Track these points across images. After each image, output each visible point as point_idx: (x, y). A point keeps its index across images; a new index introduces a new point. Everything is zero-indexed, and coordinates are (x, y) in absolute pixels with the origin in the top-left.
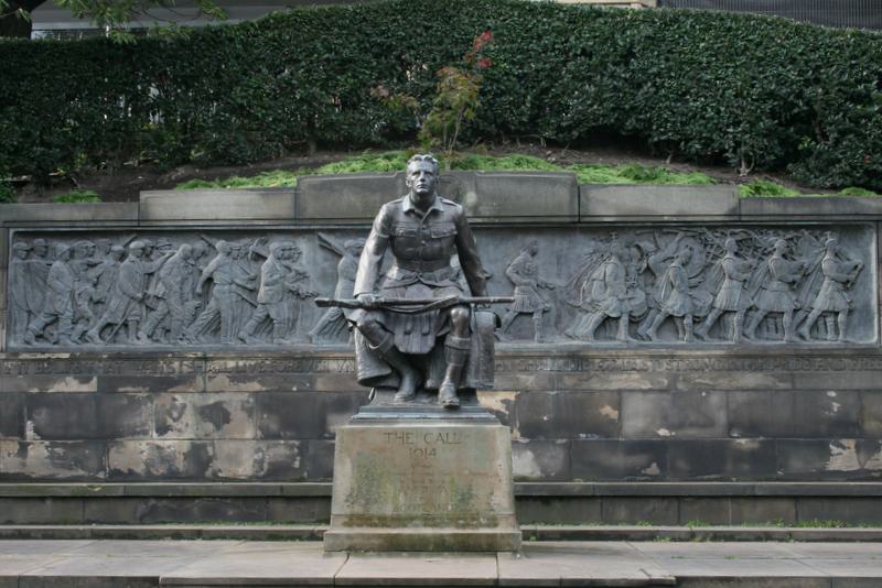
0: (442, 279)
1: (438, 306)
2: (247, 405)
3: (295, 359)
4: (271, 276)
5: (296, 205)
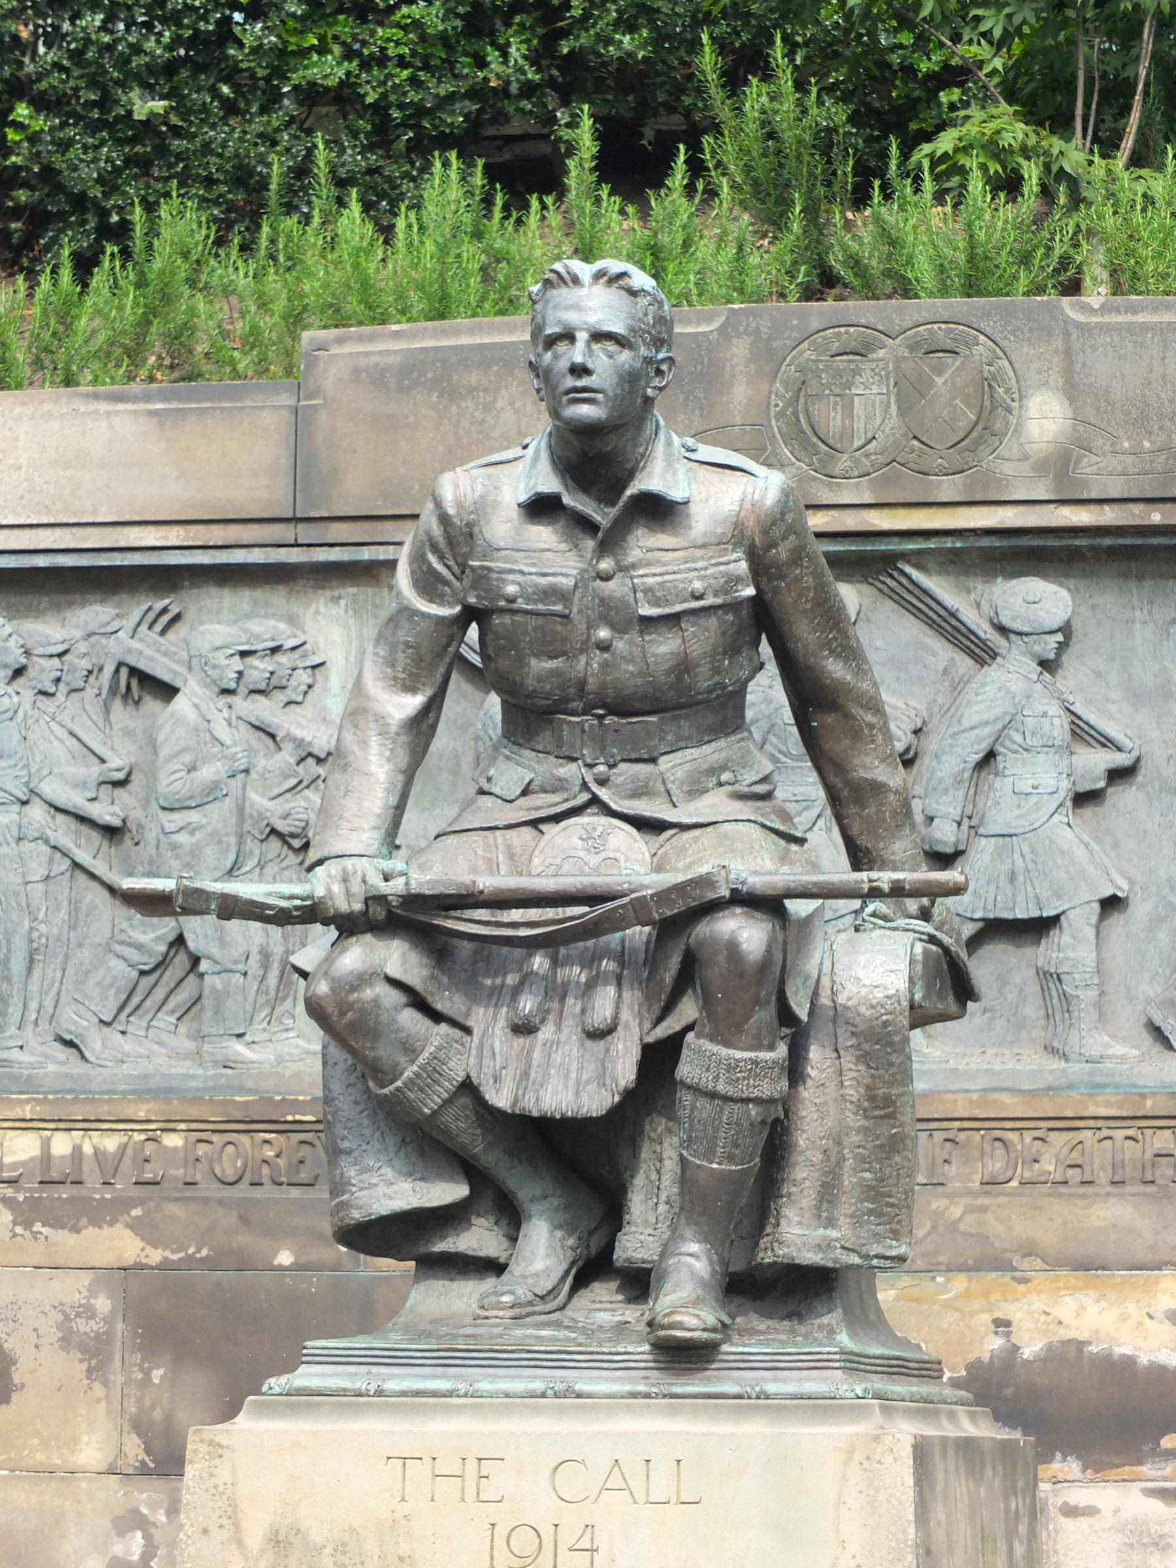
0: (696, 791)
1: (639, 911)
2: (83, 1326)
3: (287, 1129)
4: (192, 769)
5: (302, 464)
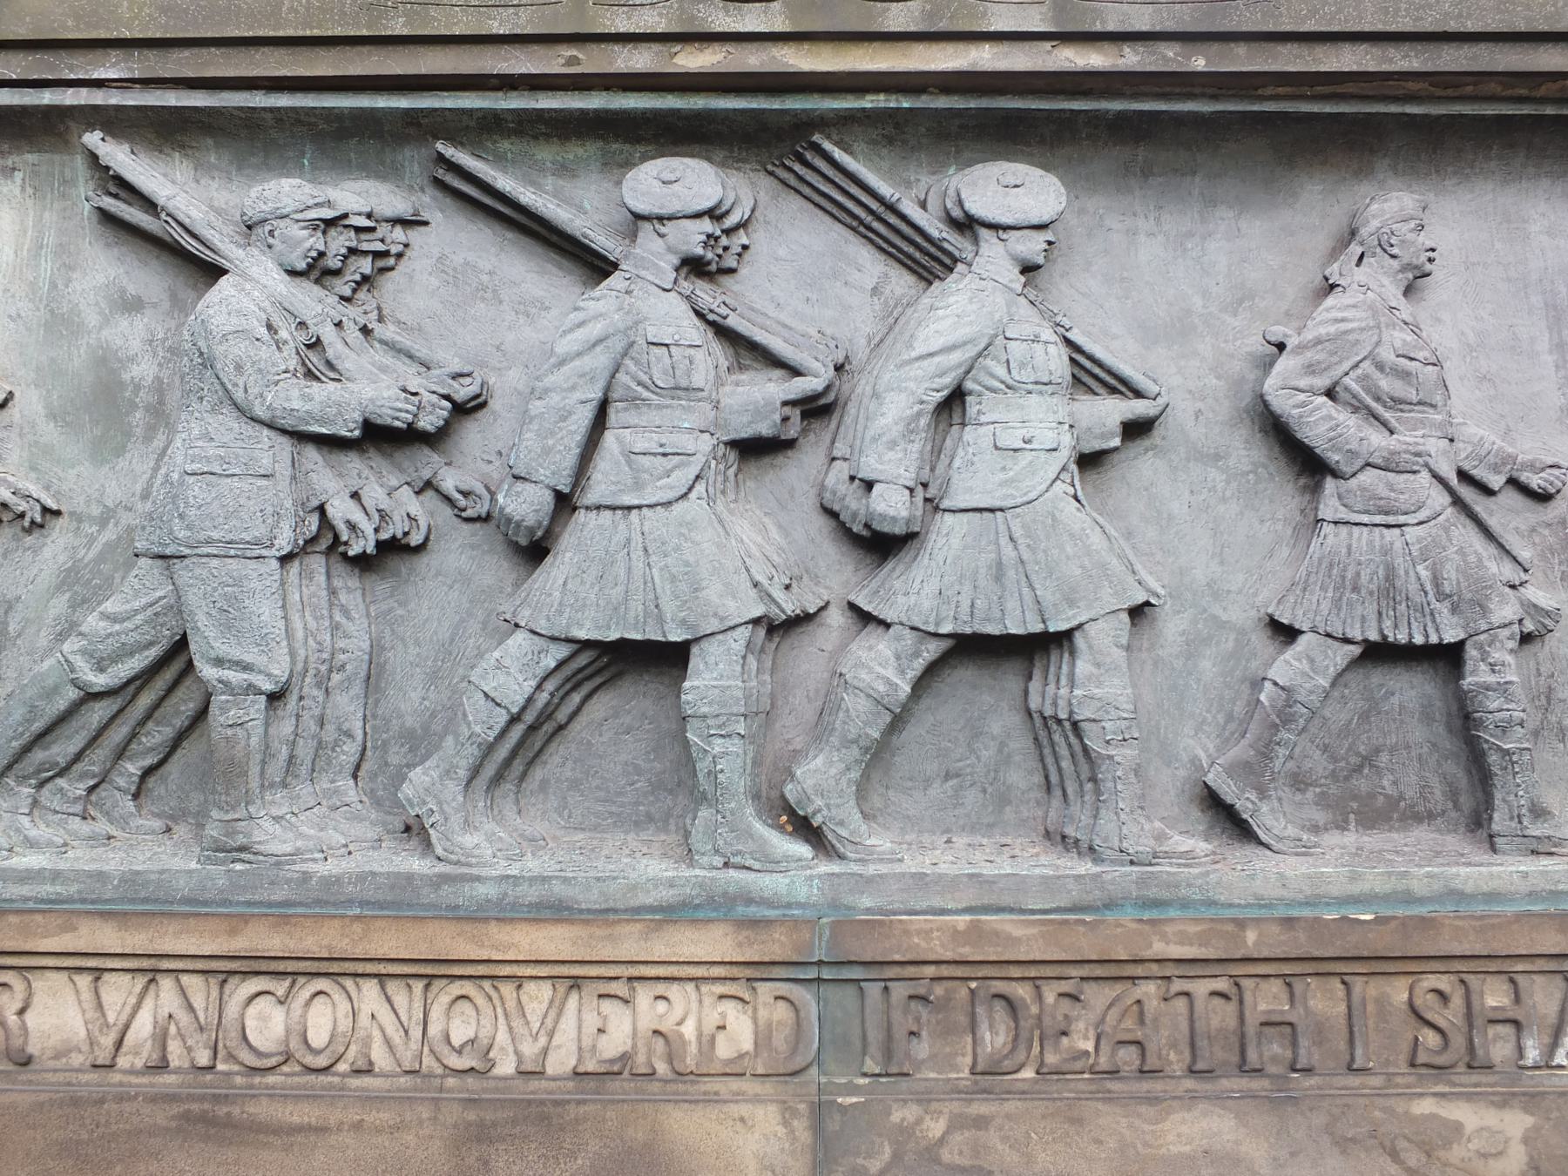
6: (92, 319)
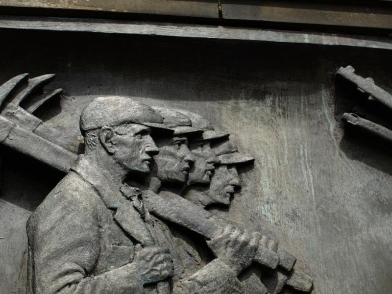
4: (90, 271)
6: (359, 216)
